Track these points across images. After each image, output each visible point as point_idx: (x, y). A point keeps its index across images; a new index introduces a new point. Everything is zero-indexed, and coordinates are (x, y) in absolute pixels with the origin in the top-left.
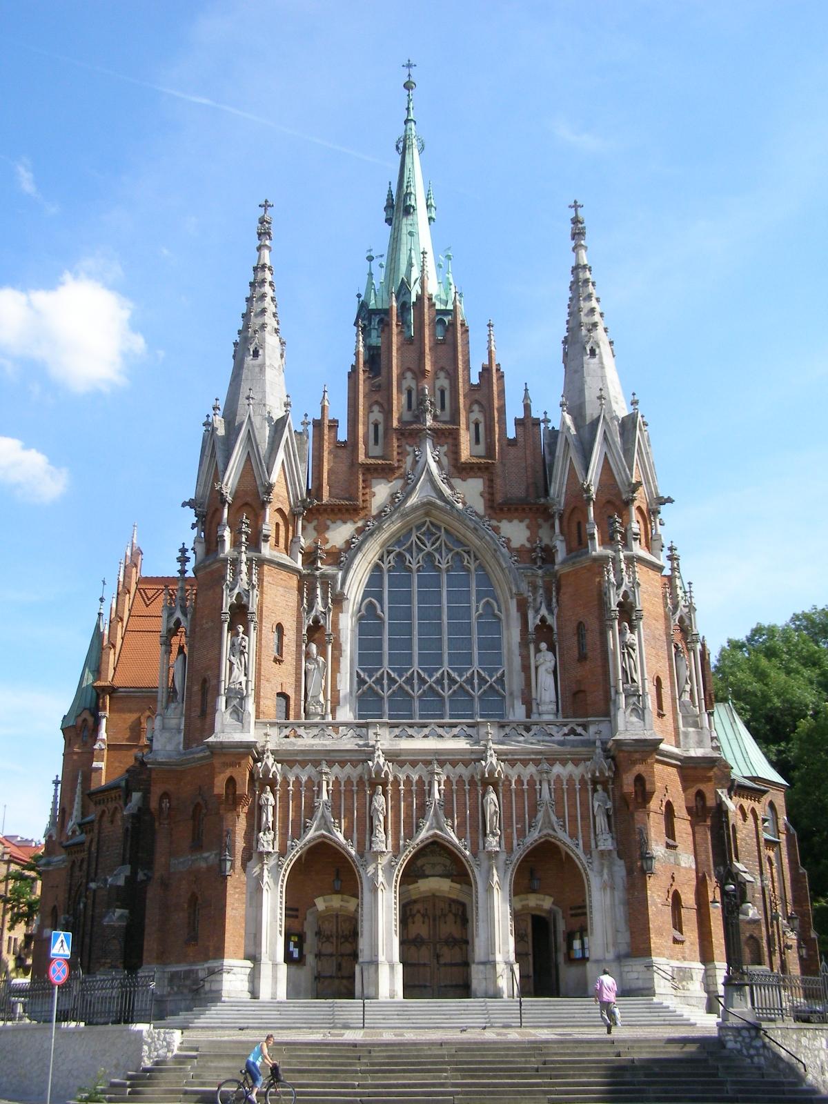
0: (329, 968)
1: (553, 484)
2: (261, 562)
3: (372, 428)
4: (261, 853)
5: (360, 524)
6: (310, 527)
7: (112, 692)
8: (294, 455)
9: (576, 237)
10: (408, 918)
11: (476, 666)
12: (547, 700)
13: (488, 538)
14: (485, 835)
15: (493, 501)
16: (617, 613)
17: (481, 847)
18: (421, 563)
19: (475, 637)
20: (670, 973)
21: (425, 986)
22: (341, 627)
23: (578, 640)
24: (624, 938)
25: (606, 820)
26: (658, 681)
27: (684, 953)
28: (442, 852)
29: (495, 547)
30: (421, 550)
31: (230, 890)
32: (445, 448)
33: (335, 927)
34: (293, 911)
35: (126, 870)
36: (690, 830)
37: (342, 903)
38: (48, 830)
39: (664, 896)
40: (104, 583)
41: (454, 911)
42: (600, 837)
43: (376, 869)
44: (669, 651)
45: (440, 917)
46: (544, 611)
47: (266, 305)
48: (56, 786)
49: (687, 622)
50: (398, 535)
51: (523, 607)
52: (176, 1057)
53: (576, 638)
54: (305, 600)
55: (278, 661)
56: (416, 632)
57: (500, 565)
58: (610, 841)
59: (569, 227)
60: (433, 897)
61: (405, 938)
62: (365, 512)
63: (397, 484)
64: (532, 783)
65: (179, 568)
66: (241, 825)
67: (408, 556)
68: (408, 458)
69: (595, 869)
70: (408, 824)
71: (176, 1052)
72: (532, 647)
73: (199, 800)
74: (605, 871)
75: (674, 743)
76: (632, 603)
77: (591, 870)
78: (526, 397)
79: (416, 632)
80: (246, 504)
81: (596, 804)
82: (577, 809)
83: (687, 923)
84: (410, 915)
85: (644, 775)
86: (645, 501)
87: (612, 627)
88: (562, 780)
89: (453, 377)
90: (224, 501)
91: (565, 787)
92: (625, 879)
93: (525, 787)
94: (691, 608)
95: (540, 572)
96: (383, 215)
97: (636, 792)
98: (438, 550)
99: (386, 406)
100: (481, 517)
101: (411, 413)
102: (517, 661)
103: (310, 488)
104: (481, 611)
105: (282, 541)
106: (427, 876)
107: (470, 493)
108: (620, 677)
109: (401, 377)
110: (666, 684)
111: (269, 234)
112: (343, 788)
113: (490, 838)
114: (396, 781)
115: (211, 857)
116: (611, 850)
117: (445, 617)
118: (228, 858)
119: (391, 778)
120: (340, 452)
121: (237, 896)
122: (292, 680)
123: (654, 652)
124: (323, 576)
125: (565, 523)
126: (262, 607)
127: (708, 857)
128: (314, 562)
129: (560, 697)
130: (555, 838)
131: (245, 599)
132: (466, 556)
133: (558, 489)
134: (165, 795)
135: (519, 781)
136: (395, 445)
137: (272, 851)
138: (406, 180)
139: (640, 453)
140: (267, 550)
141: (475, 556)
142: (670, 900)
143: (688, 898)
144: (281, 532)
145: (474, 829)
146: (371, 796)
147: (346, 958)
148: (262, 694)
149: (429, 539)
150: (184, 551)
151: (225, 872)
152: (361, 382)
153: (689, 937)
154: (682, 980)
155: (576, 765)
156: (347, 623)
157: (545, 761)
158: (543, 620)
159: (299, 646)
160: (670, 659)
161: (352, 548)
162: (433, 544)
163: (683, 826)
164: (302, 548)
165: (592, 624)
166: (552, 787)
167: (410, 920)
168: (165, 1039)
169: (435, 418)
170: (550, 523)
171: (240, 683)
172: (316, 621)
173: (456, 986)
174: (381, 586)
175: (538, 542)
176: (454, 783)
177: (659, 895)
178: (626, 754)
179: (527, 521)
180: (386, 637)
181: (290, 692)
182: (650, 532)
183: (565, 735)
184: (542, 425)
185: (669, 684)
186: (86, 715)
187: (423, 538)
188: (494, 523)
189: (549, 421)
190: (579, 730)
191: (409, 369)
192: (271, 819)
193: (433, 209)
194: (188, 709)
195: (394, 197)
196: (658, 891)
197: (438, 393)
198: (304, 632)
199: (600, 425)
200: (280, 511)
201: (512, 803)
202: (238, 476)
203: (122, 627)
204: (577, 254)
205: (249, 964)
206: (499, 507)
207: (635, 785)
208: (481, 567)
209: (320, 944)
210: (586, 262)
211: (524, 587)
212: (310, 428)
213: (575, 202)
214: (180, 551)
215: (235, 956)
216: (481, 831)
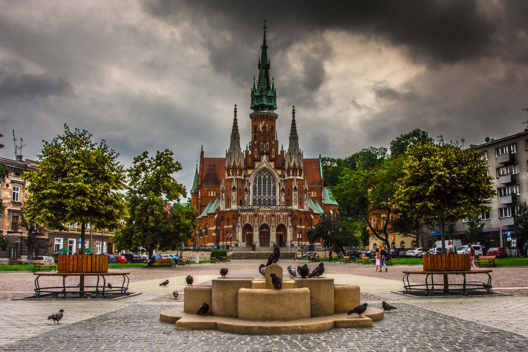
24: (292, 239)
26: (300, 199)
55: (240, 195)
60: (264, 232)
63: (260, 163)
64: (279, 215)
96: (258, 66)
107: (272, 164)
110: (302, 199)
133: (286, 166)
134: (223, 216)
156: (251, 187)
165: (290, 189)
181: (242, 200)
186: (196, 191)
206: (276, 168)
208: (273, 178)
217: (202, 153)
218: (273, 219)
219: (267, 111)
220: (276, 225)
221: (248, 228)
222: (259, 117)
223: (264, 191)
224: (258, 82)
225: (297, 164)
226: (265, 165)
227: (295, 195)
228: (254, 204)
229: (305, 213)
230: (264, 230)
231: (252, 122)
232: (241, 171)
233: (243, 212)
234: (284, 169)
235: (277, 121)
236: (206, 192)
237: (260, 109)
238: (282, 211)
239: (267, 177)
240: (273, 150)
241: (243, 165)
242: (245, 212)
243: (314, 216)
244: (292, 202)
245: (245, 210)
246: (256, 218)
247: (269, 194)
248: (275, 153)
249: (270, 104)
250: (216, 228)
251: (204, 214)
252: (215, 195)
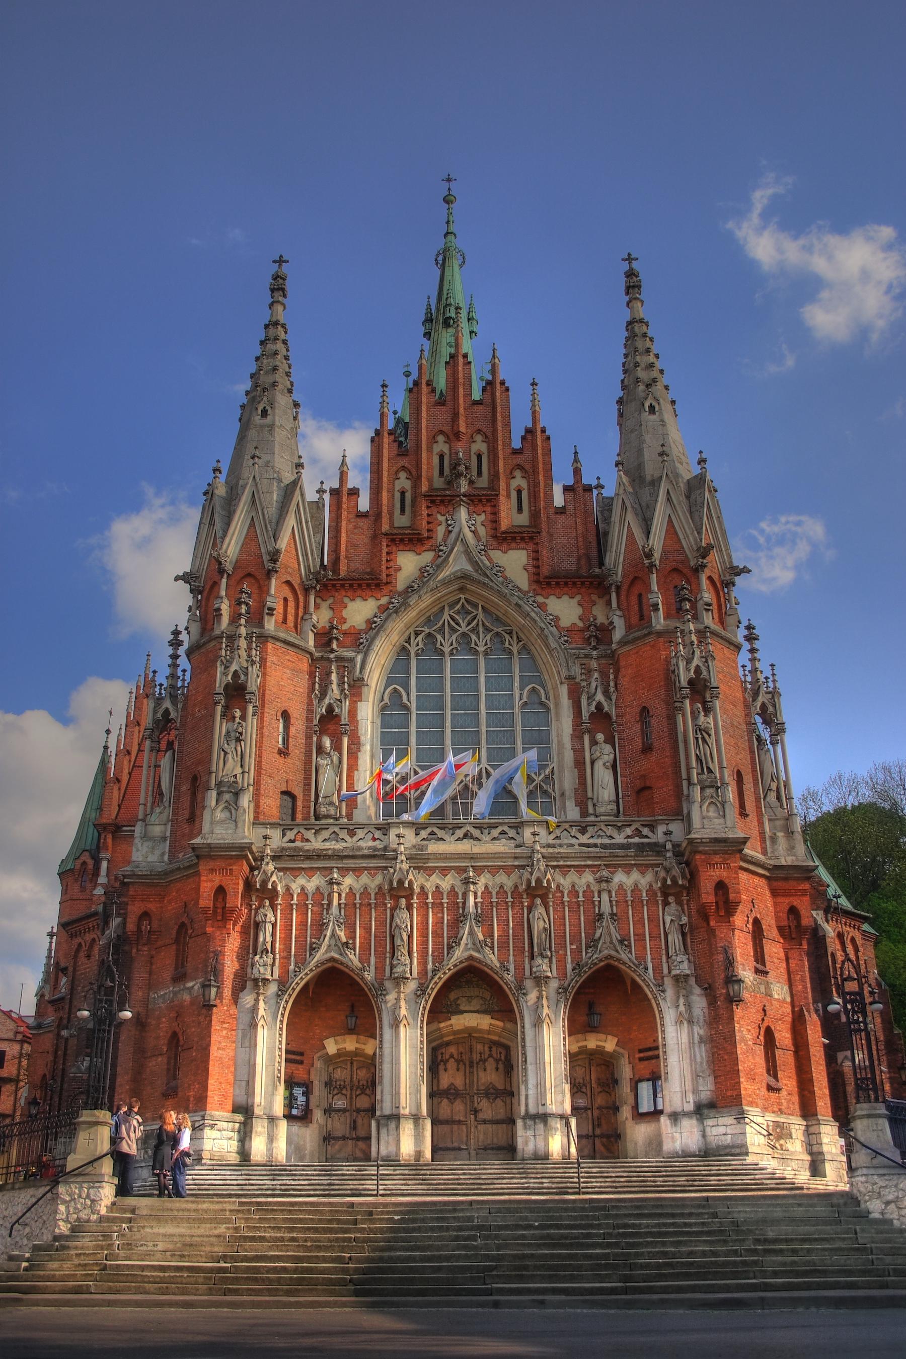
0: (339, 1126)
1: (608, 554)
2: (263, 638)
3: (398, 495)
4: (256, 981)
5: (384, 600)
6: (325, 605)
7: (116, 831)
8: (307, 522)
9: (631, 291)
10: (438, 1065)
12: (606, 798)
13: (533, 614)
14: (532, 957)
15: (538, 574)
16: (688, 691)
17: (527, 973)
18: (455, 645)
19: (519, 728)
20: (764, 1127)
21: (460, 1149)
22: (359, 717)
23: (642, 730)
25: (680, 937)
26: (739, 774)
27: (779, 1104)
28: (480, 982)
29: (543, 626)
30: (456, 631)
31: (216, 1026)
32: (483, 517)
33: (349, 1077)
34: (294, 1056)
36: (782, 955)
37: (358, 1046)
38: (41, 988)
39: (755, 1032)
40: (111, 713)
41: (495, 1055)
42: (674, 958)
43: (398, 999)
44: (750, 742)
45: (477, 1063)
46: (600, 697)
47: (278, 363)
48: (51, 939)
49: (771, 709)
50: (428, 614)
51: (575, 695)
52: (101, 1219)
53: (639, 726)
54: (317, 686)
56: (448, 723)
57: (547, 646)
58: (686, 963)
59: (622, 281)
61: (435, 1088)
62: (390, 588)
63: (428, 557)
64: (588, 893)
65: (171, 652)
66: (232, 943)
67: (439, 638)
68: (439, 528)
69: (668, 999)
70: (438, 945)
71: (103, 1211)
72: (586, 738)
73: (184, 919)
74: (682, 1001)
75: (759, 849)
76: (705, 680)
77: (664, 999)
78: (576, 460)
79: (448, 723)
80: (249, 575)
81: (668, 919)
82: (644, 926)
83: (783, 1067)
84: (442, 1061)
85: (726, 881)
86: (716, 571)
87: (682, 709)
88: (625, 891)
89: (491, 440)
90: (221, 571)
91: (629, 898)
92: (706, 1011)
93: (581, 899)
94: (774, 694)
95: (595, 653)
96: (422, 330)
97: (717, 903)
98: (475, 630)
99: (414, 473)
100: (525, 593)
101: (442, 479)
102: (569, 756)
103: (326, 563)
104: (525, 699)
105: (291, 618)
106: (462, 1012)
108: (694, 766)
109: (433, 440)
110: (748, 779)
111: (283, 290)
112: (358, 901)
113: (539, 961)
114: (423, 892)
115: (196, 987)
116: (688, 975)
117: (483, 706)
118: (213, 983)
119: (417, 890)
120: (362, 522)
121: (224, 1032)
122: (300, 777)
123: (733, 741)
124: (339, 659)
125: (623, 597)
126: (264, 691)
127: (806, 988)
128: (329, 643)
129: (620, 796)
130: (619, 960)
131: (242, 677)
132: (507, 637)
134: (146, 915)
135: (574, 892)
136: (425, 513)
137: (269, 977)
138: (445, 292)
139: (710, 516)
140: (270, 625)
141: (518, 637)
142: (761, 1038)
143: (784, 1036)
144: (289, 609)
145: (519, 950)
146: (393, 909)
147: (363, 1114)
148: (262, 792)
149: (463, 620)
150: (176, 633)
151: (209, 1000)
152: (386, 446)
153: (786, 1085)
154: (779, 1137)
155: (643, 873)
157: (603, 867)
158: (599, 706)
159: (308, 738)
160: (752, 752)
161: (373, 627)
162: (469, 624)
163: (774, 949)
164: (314, 626)
166: (614, 898)
167: (441, 1067)
168: (88, 1196)
169: (471, 482)
170: (607, 597)
171: (235, 776)
172: (330, 709)
173: (499, 1148)
174: (408, 671)
175: (592, 619)
176: (494, 895)
177: (749, 1031)
178: (703, 857)
179: (578, 597)
180: (413, 729)
181: (298, 792)
182: (723, 606)
183: (628, 837)
184: (595, 492)
185: (751, 780)
186: (86, 857)
187: (457, 617)
188: (540, 599)
189: (602, 487)
190: (645, 831)
191: (441, 432)
192: (269, 939)
193: (474, 322)
194: (175, 813)
195: (433, 312)
196: (748, 1024)
197: (474, 459)
198: (316, 722)
199: (662, 484)
200: (288, 583)
201: (565, 919)
202: (240, 544)
203: (130, 761)
204: (632, 309)
205: (239, 1118)
207: (716, 895)
208: (525, 649)
209: (330, 1096)
210: (642, 316)
211: (576, 670)
212: (327, 497)
213: (629, 255)
214: (173, 633)
215: (221, 1107)
216: (527, 954)
220: (562, 975)
225: (688, 542)
233: (295, 872)
239: (481, 643)
242: (311, 872)
245: (320, 855)
246: (402, 916)
248: (534, 496)
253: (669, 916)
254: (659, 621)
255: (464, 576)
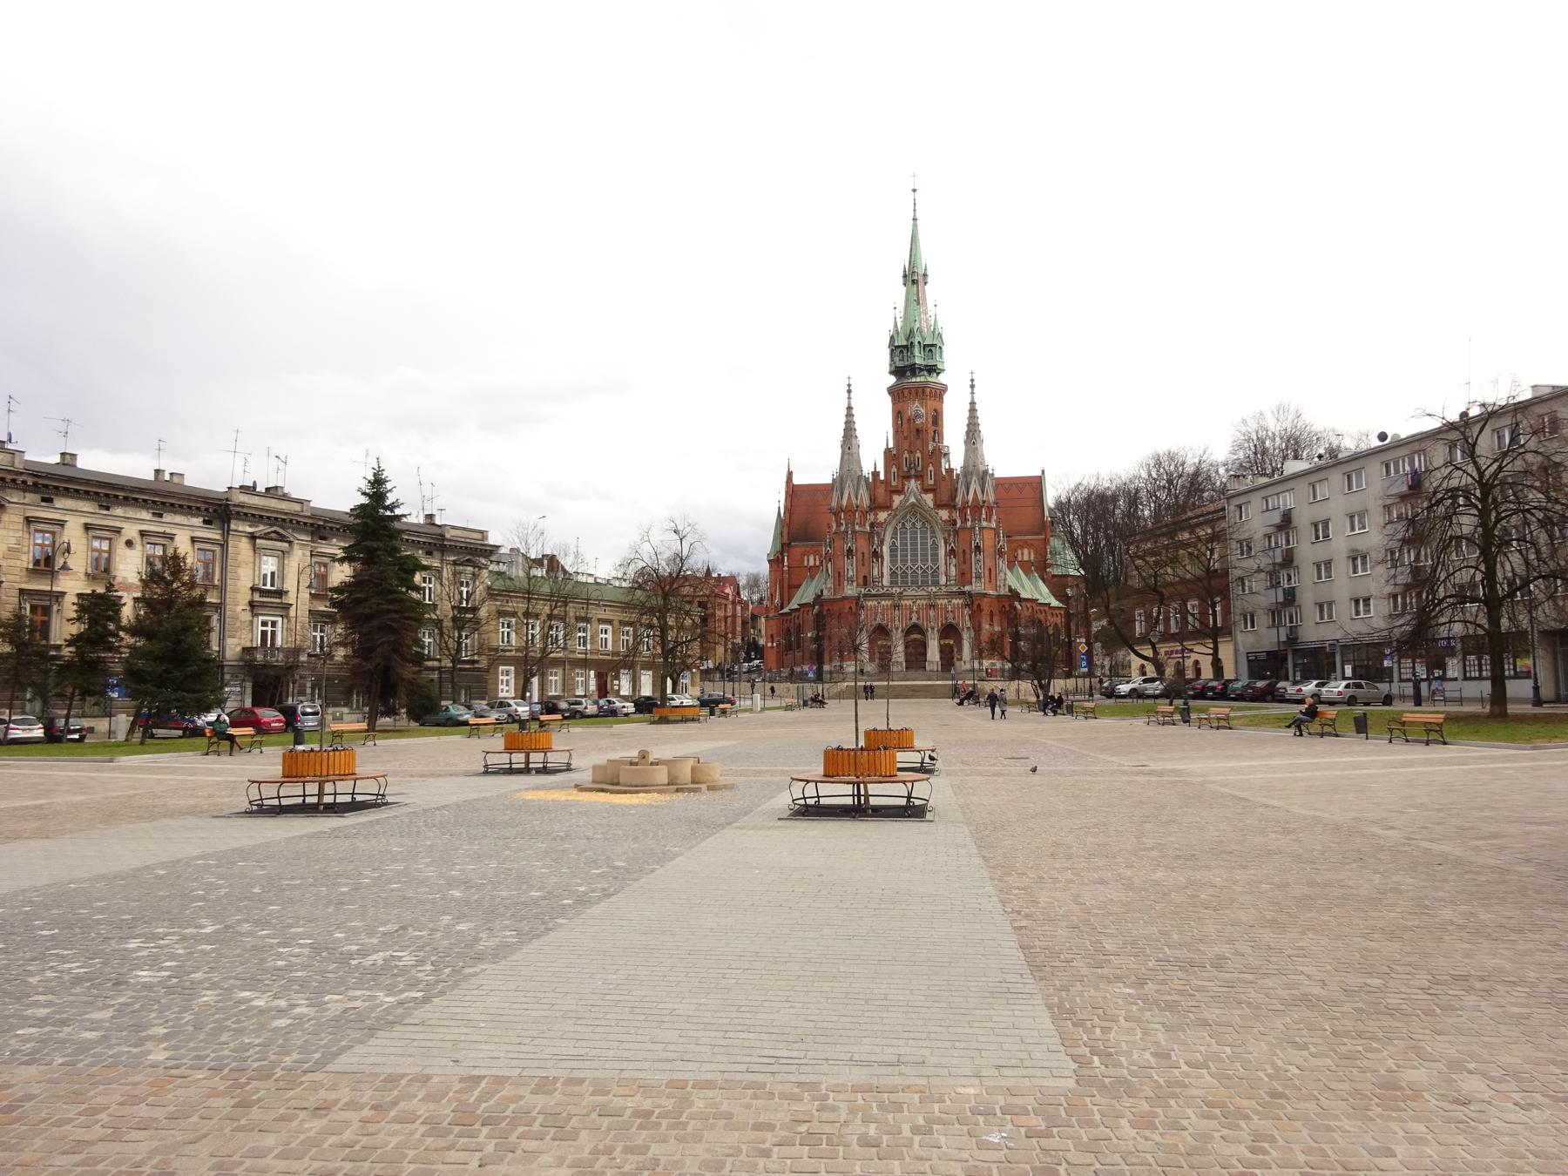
11: (929, 563)
35: (815, 632)
55: (863, 565)
63: (902, 496)
102: (944, 562)
107: (929, 499)
133: (959, 500)
134: (829, 610)
156: (886, 549)
165: (967, 551)
206: (938, 506)
217: (790, 474)
218: (932, 613)
219: (922, 379)
221: (882, 631)
222: (906, 392)
223: (914, 555)
224: (902, 315)
226: (912, 500)
227: (978, 563)
228: (893, 583)
229: (999, 597)
230: (915, 636)
231: (894, 404)
232: (864, 514)
234: (954, 507)
235: (946, 397)
236: (799, 557)
237: (908, 374)
238: (951, 595)
239: (919, 525)
240: (931, 468)
241: (866, 503)
243: (1023, 604)
244: (971, 577)
245: (875, 595)
246: (897, 612)
247: (924, 561)
249: (930, 362)
250: (817, 635)
251: (794, 605)
252: (818, 563)
253: (967, 611)
254: (969, 524)
255: (913, 505)
